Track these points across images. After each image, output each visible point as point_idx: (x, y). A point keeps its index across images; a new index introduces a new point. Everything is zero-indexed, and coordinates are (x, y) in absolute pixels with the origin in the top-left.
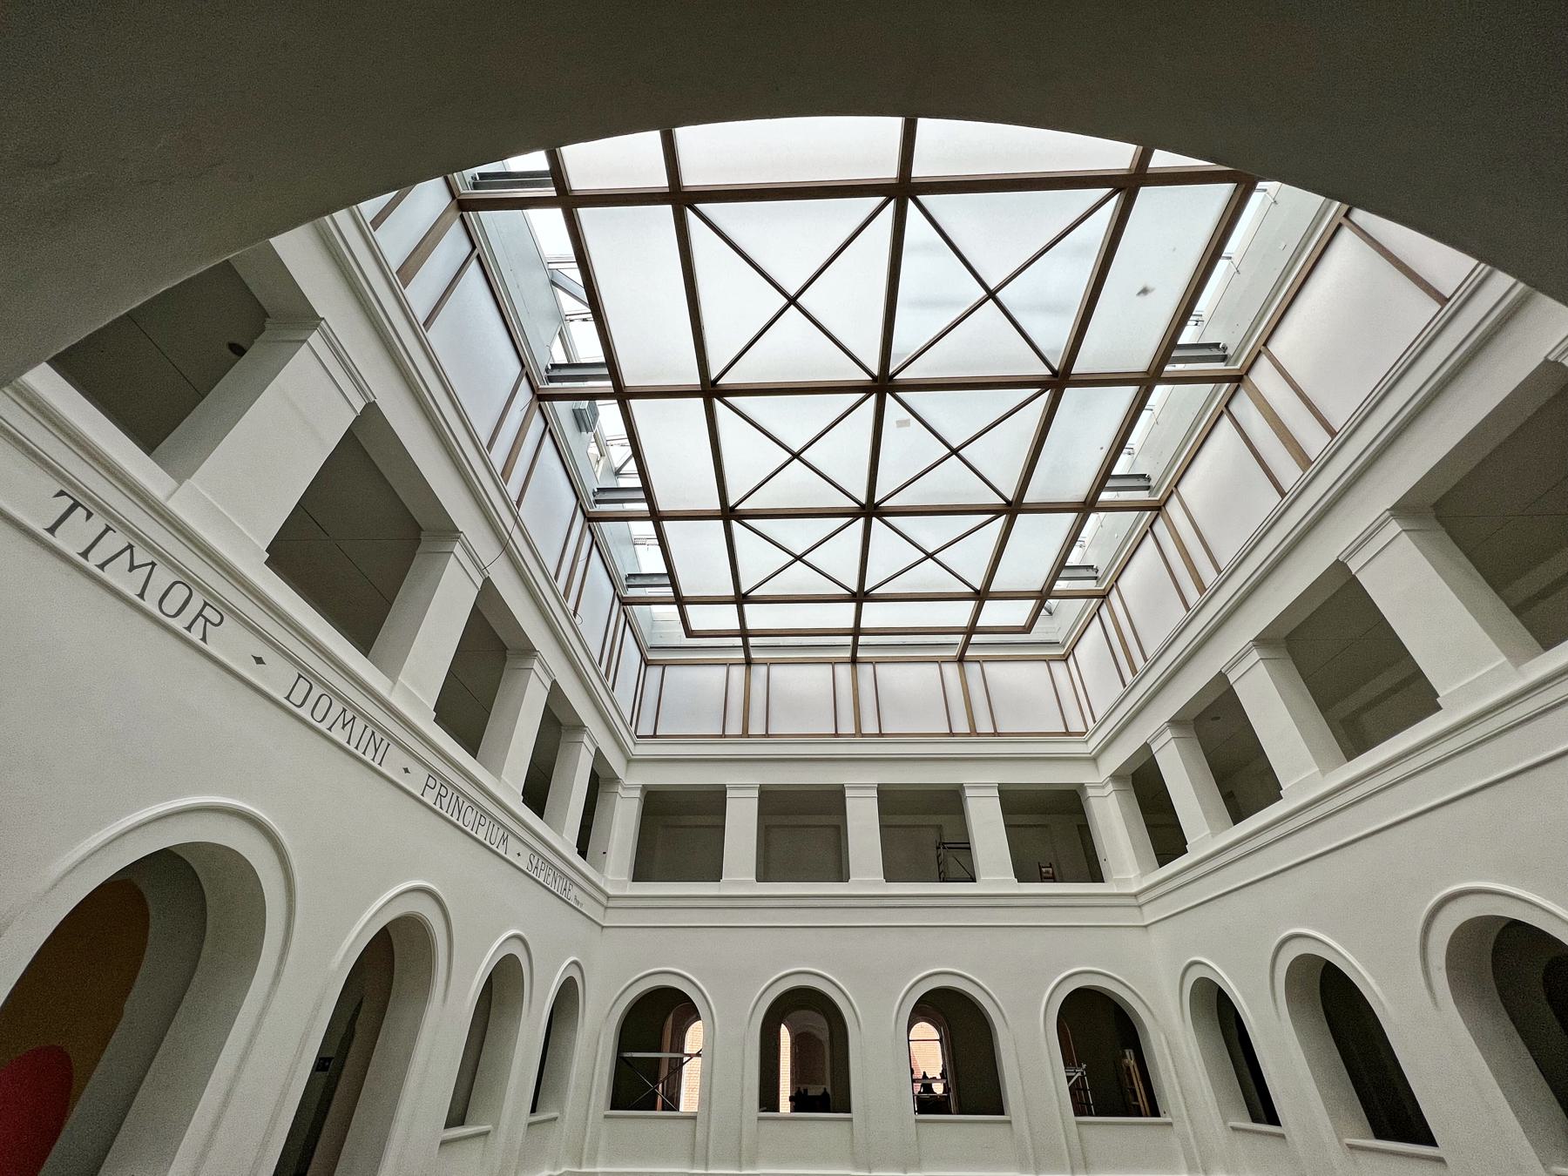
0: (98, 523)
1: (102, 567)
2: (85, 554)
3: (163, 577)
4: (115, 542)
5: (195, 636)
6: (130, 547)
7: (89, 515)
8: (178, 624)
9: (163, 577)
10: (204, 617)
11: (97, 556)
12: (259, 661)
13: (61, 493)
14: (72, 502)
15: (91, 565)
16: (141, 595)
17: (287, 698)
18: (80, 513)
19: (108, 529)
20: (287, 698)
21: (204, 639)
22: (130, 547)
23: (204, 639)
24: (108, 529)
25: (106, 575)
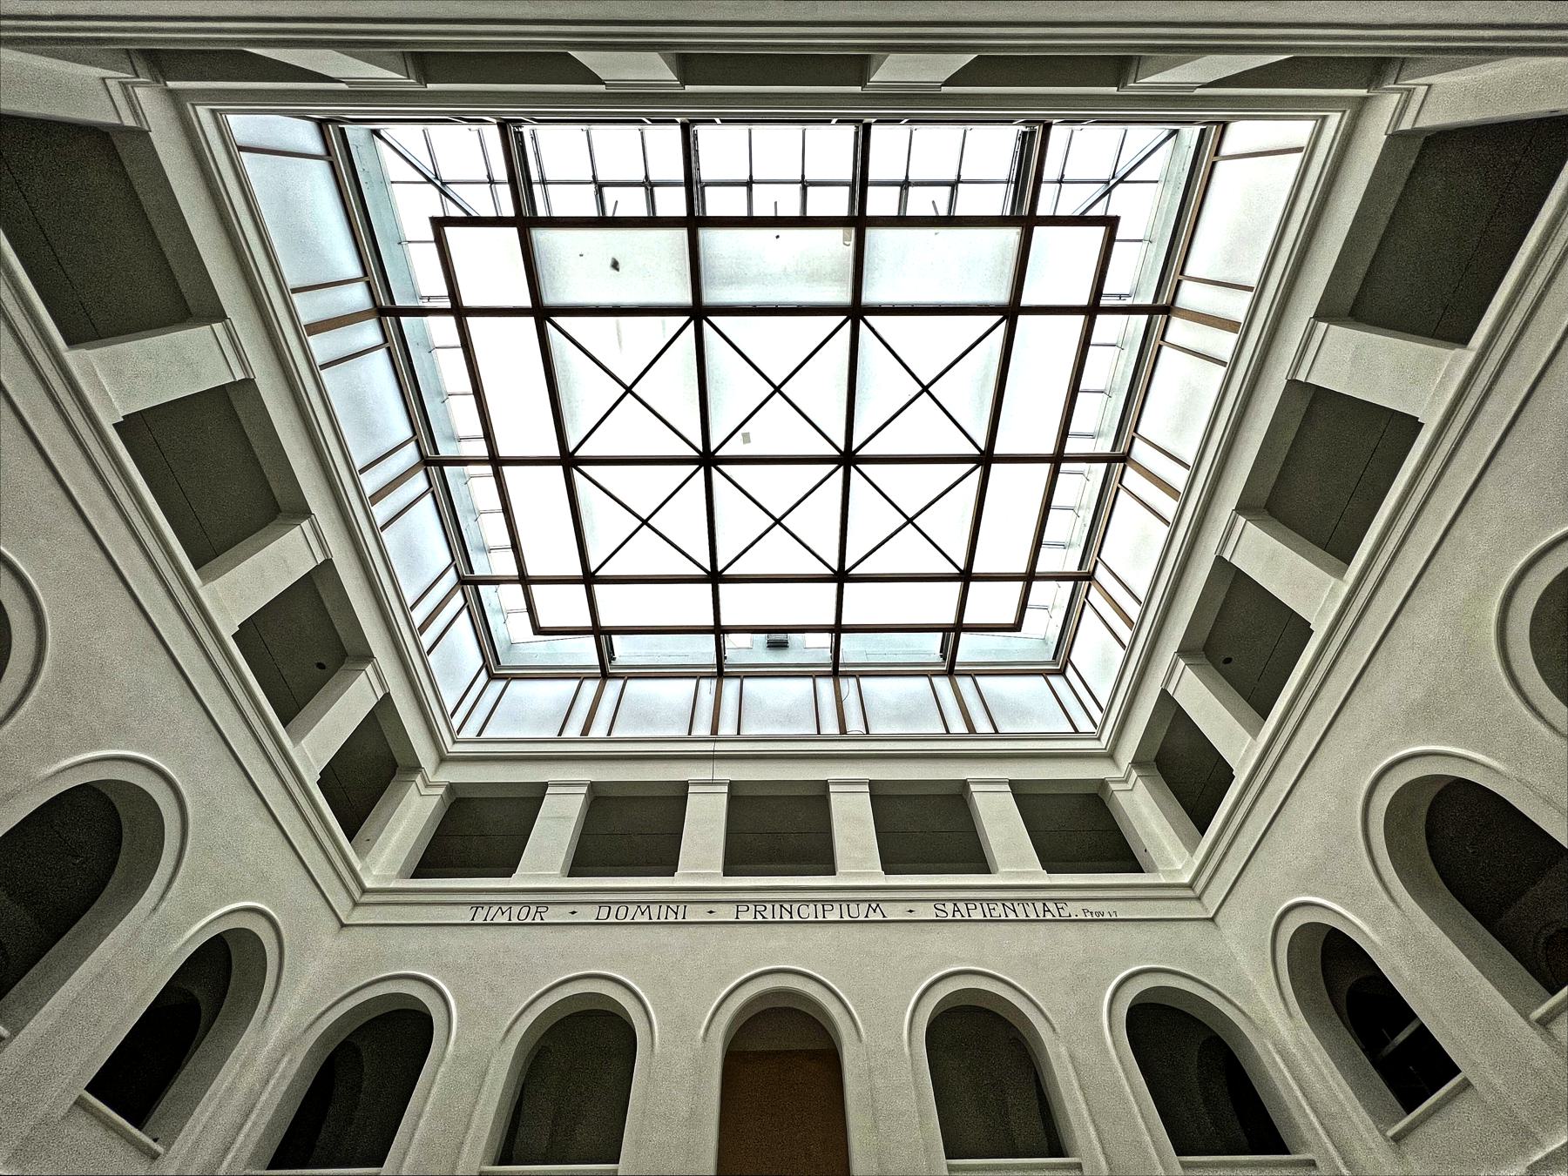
2: (485, 920)
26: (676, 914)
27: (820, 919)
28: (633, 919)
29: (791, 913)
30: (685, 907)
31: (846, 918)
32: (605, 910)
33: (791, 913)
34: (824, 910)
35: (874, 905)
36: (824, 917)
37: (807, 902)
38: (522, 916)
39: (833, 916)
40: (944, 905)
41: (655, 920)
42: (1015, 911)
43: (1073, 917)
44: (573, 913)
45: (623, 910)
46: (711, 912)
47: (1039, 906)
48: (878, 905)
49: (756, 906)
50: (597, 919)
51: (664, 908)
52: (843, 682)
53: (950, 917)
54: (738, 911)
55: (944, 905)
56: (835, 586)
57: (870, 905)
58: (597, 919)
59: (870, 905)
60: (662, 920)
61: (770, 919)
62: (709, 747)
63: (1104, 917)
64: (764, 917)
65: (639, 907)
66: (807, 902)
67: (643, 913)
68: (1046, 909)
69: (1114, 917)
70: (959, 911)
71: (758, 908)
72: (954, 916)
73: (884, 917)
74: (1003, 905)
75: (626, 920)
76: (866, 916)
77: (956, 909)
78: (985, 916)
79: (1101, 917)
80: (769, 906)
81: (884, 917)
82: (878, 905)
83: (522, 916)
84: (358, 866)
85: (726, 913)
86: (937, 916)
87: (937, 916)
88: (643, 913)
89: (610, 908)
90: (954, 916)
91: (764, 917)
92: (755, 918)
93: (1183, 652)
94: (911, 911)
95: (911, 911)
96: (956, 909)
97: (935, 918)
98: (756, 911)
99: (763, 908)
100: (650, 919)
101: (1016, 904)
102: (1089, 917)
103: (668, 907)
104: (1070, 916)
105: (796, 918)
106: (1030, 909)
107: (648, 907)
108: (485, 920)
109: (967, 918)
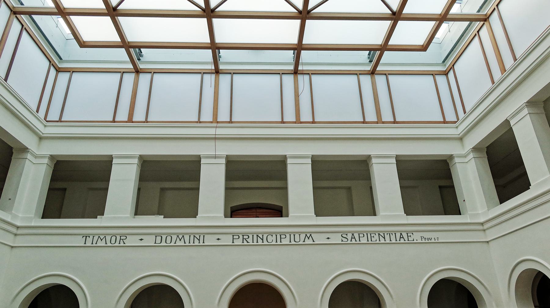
0: (91, 237)
1: (96, 244)
2: (92, 244)
3: (108, 238)
4: (96, 238)
5: (122, 244)
6: (99, 237)
7: (89, 237)
8: (117, 244)
9: (108, 238)
11: (94, 242)
13: (83, 237)
14: (85, 237)
15: (94, 245)
16: (106, 244)
18: (88, 237)
19: (93, 237)
21: (124, 243)
22: (99, 237)
23: (124, 243)
24: (93, 237)
25: (98, 245)
26: (199, 240)
27: (279, 243)
28: (175, 243)
29: (262, 240)
30: (204, 236)
31: (293, 243)
32: (159, 239)
33: (262, 240)
35: (308, 235)
36: (281, 242)
37: (271, 234)
38: (113, 241)
39: (285, 241)
40: (347, 234)
41: (187, 244)
42: (384, 238)
43: (415, 241)
44: (141, 240)
45: (169, 239)
46: (218, 239)
47: (398, 235)
49: (243, 236)
50: (155, 243)
51: (192, 237)
52: (300, 77)
53: (349, 242)
54: (233, 239)
55: (347, 234)
56: (298, 22)
57: (306, 235)
58: (155, 243)
59: (306, 235)
60: (192, 244)
61: (251, 243)
62: (211, 132)
63: (431, 241)
64: (248, 242)
65: (177, 236)
66: (271, 234)
67: (180, 240)
68: (402, 237)
69: (437, 241)
72: (351, 241)
73: (314, 241)
74: (379, 234)
75: (171, 244)
76: (304, 241)
77: (353, 237)
78: (368, 241)
79: (430, 241)
80: (251, 236)
81: (314, 241)
83: (113, 241)
84: (9, 219)
85: (227, 240)
86: (342, 241)
87: (342, 241)
88: (180, 240)
90: (351, 241)
91: (248, 242)
92: (243, 242)
93: (531, 103)
94: (328, 238)
95: (328, 238)
96: (353, 237)
97: (341, 242)
99: (247, 237)
100: (185, 243)
101: (386, 234)
102: (424, 241)
103: (194, 236)
104: (413, 240)
105: (266, 243)
106: (393, 237)
108: (92, 244)
109: (358, 242)
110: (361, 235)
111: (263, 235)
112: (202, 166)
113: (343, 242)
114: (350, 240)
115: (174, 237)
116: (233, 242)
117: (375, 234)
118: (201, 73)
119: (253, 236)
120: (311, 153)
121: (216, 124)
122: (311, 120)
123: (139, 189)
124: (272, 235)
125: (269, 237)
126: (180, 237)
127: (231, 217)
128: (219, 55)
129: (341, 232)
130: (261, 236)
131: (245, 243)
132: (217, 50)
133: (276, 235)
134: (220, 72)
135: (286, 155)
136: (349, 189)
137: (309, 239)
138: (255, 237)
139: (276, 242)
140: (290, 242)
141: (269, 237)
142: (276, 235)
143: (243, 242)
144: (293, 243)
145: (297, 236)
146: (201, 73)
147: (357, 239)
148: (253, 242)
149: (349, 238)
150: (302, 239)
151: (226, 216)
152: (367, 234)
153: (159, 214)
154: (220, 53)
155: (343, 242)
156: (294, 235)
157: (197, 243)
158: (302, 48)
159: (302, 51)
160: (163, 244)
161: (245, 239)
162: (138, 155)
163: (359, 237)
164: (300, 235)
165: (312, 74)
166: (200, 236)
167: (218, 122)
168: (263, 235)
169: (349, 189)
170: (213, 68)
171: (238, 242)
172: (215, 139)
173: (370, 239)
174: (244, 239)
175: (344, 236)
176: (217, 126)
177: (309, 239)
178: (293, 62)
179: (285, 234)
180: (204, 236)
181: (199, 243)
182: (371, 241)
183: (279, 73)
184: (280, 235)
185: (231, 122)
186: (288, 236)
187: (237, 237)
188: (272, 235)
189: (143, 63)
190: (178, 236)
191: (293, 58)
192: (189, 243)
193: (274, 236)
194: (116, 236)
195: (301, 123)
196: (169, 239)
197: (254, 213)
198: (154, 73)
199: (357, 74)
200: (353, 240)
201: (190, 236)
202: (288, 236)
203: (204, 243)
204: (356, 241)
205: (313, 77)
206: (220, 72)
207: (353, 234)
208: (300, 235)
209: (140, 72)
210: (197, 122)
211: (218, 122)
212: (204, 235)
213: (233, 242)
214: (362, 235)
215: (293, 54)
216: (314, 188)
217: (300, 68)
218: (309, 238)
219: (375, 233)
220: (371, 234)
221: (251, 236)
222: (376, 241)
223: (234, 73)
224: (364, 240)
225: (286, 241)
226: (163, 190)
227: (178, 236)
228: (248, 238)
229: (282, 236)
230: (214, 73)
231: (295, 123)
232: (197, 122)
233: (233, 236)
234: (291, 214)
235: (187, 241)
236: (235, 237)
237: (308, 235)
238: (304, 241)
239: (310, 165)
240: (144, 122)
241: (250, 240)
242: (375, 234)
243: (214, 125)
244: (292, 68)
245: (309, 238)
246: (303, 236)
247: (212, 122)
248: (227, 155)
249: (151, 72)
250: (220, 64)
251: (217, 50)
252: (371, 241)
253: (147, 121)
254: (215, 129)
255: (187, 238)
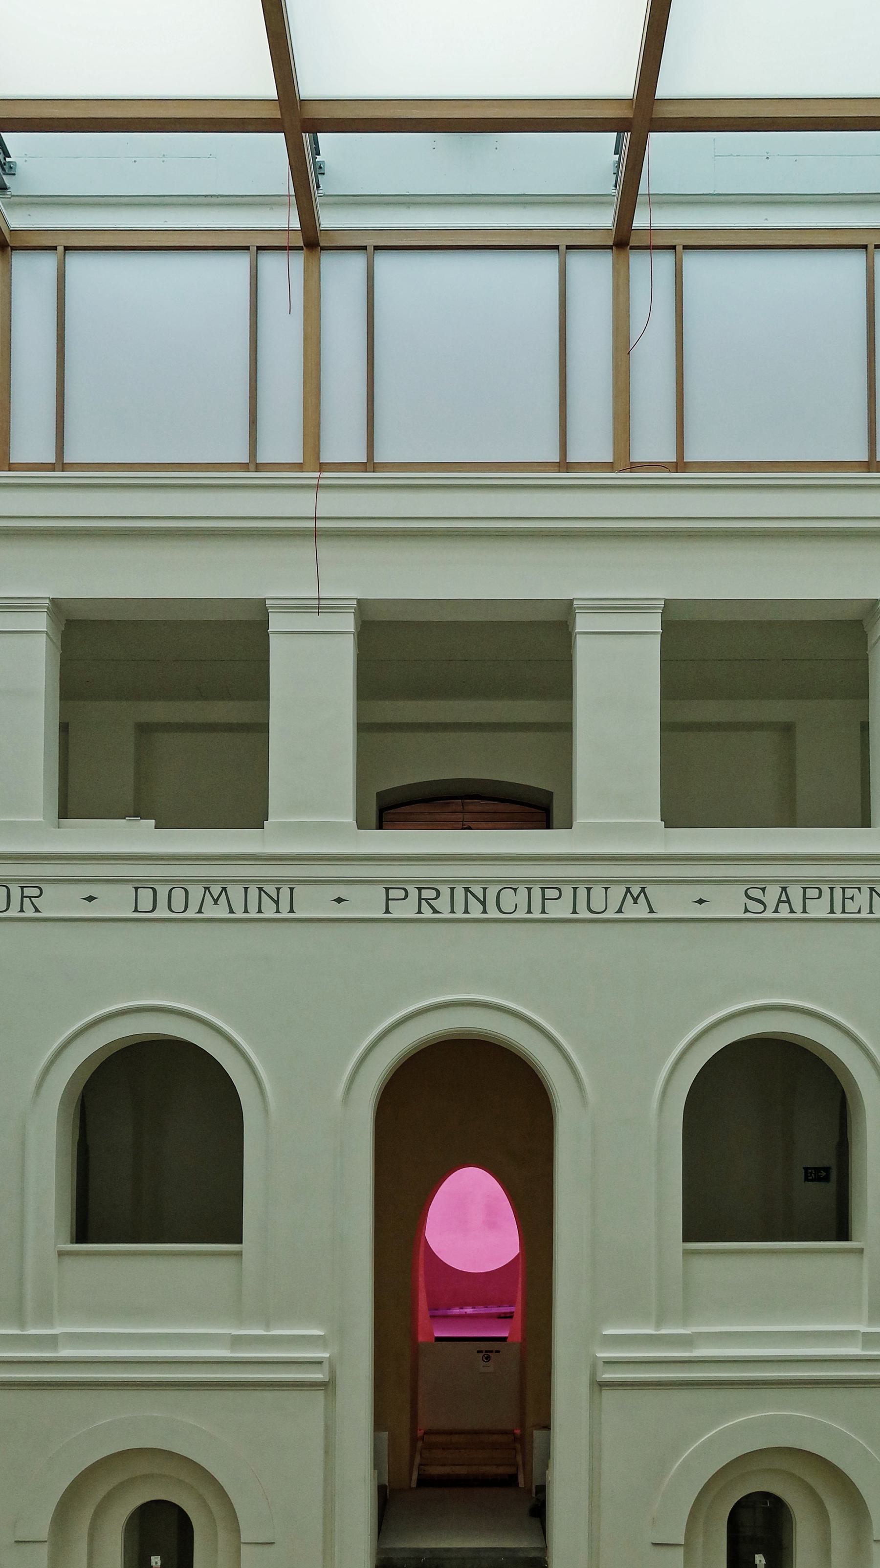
10: (26, 897)
12: (90, 899)
17: (136, 910)
20: (136, 910)
26: (277, 902)
27: (537, 914)
28: (200, 912)
29: (483, 903)
30: (292, 889)
31: (584, 914)
32: (146, 896)
33: (483, 903)
34: (544, 899)
35: (636, 890)
36: (543, 912)
40: (763, 889)
41: (240, 914)
45: (178, 896)
46: (339, 900)
48: (643, 890)
49: (420, 889)
51: (253, 892)
53: (769, 914)
54: (388, 899)
55: (763, 889)
57: (628, 890)
59: (628, 890)
64: (435, 911)
67: (216, 902)
70: (788, 901)
71: (426, 894)
73: (652, 911)
76: (620, 911)
77: (784, 898)
80: (445, 891)
81: (652, 911)
82: (643, 890)
86: (746, 911)
87: (746, 911)
88: (216, 902)
89: (154, 891)
91: (435, 911)
92: (420, 912)
94: (701, 901)
98: (420, 899)
99: (432, 894)
100: (231, 911)
103: (260, 889)
105: (493, 913)
107: (224, 889)
110: (812, 893)
111: (485, 889)
112: (274, 641)
113: (748, 915)
114: (771, 907)
115: (196, 892)
116: (387, 911)
117: (859, 889)
118: (247, 248)
119: (452, 889)
120: (662, 592)
121: (317, 475)
122: (671, 457)
123: (64, 728)
124: (515, 890)
125: (507, 894)
126: (216, 890)
127: (380, 827)
128: (314, 159)
129: (745, 881)
130: (478, 890)
131: (427, 913)
132: (306, 137)
133: (529, 889)
134: (322, 244)
135: (572, 601)
136: (787, 729)
137: (635, 902)
138: (460, 892)
139: (529, 912)
140: (574, 912)
141: (507, 894)
142: (529, 889)
143: (420, 912)
144: (584, 914)
145: (598, 892)
146: (247, 248)
147: (797, 905)
148: (453, 912)
149: (771, 903)
150: (615, 905)
151: (361, 825)
152: (832, 889)
153: (139, 813)
154: (319, 154)
155: (748, 915)
156: (589, 889)
157: (269, 911)
158: (652, 119)
159: (654, 138)
160: (162, 912)
161: (426, 900)
162: (47, 601)
163: (805, 898)
164: (606, 889)
165: (685, 247)
166: (278, 889)
167: (323, 467)
168: (485, 889)
169: (787, 729)
170: (296, 224)
171: (405, 910)
172: (316, 534)
173: (838, 907)
174: (423, 902)
175: (752, 893)
176: (321, 482)
177: (635, 902)
178: (611, 190)
179: (557, 885)
180: (292, 889)
181: (278, 911)
182: (844, 912)
183: (556, 247)
184: (543, 889)
185: (370, 465)
186: (567, 891)
187: (402, 894)
188: (515, 890)
189: (21, 204)
190: (208, 888)
191: (613, 170)
192: (246, 911)
193: (523, 891)
194: (39, 888)
195: (633, 467)
196: (178, 896)
197: (460, 816)
198: (66, 249)
199: (865, 247)
200: (784, 907)
201: (246, 889)
202: (567, 891)
203: (292, 911)
204: (792, 911)
205: (693, 263)
206: (322, 244)
207: (784, 889)
208: (606, 889)
209: (14, 249)
210: (244, 467)
211: (323, 467)
212: (293, 883)
213: (387, 911)
214: (816, 893)
215: (615, 154)
216: (667, 727)
217: (640, 221)
218: (635, 900)
219: (857, 884)
220: (844, 889)
221: (445, 891)
222: (859, 912)
223: (376, 248)
224: (818, 909)
225: (559, 909)
226: (144, 729)
227: (208, 888)
228: (436, 898)
229: (550, 893)
230: (299, 248)
231: (609, 467)
232: (244, 467)
233: (387, 889)
234: (579, 819)
235: (238, 907)
236: (393, 894)
237: (636, 890)
238: (620, 911)
239: (658, 638)
240: (51, 467)
241: (442, 904)
242: (859, 889)
243: (310, 476)
244: (606, 219)
245: (635, 900)
246: (617, 893)
247: (299, 467)
248: (359, 601)
249: (54, 248)
250: (322, 204)
251: (306, 137)
252: (844, 912)
253: (60, 464)
254: (311, 495)
255: (236, 893)
